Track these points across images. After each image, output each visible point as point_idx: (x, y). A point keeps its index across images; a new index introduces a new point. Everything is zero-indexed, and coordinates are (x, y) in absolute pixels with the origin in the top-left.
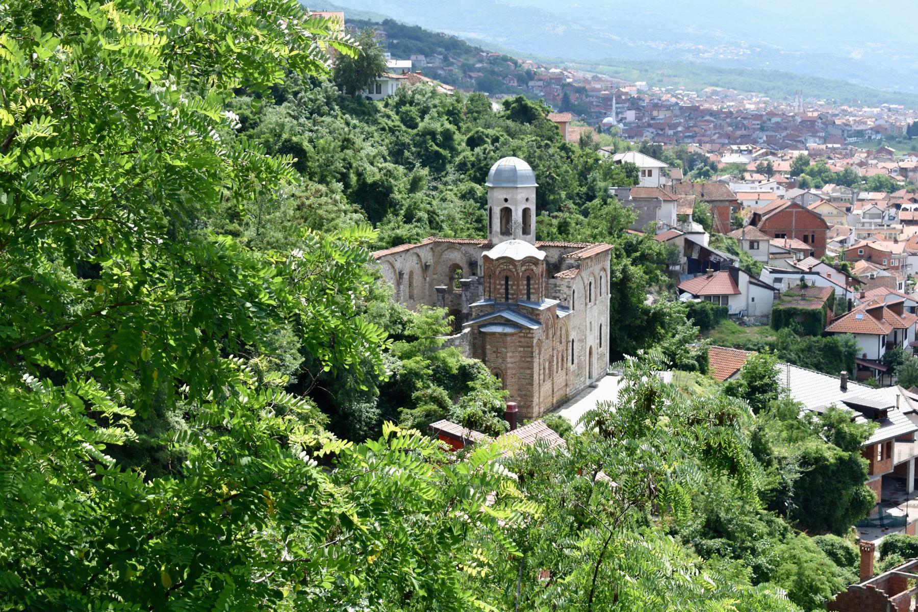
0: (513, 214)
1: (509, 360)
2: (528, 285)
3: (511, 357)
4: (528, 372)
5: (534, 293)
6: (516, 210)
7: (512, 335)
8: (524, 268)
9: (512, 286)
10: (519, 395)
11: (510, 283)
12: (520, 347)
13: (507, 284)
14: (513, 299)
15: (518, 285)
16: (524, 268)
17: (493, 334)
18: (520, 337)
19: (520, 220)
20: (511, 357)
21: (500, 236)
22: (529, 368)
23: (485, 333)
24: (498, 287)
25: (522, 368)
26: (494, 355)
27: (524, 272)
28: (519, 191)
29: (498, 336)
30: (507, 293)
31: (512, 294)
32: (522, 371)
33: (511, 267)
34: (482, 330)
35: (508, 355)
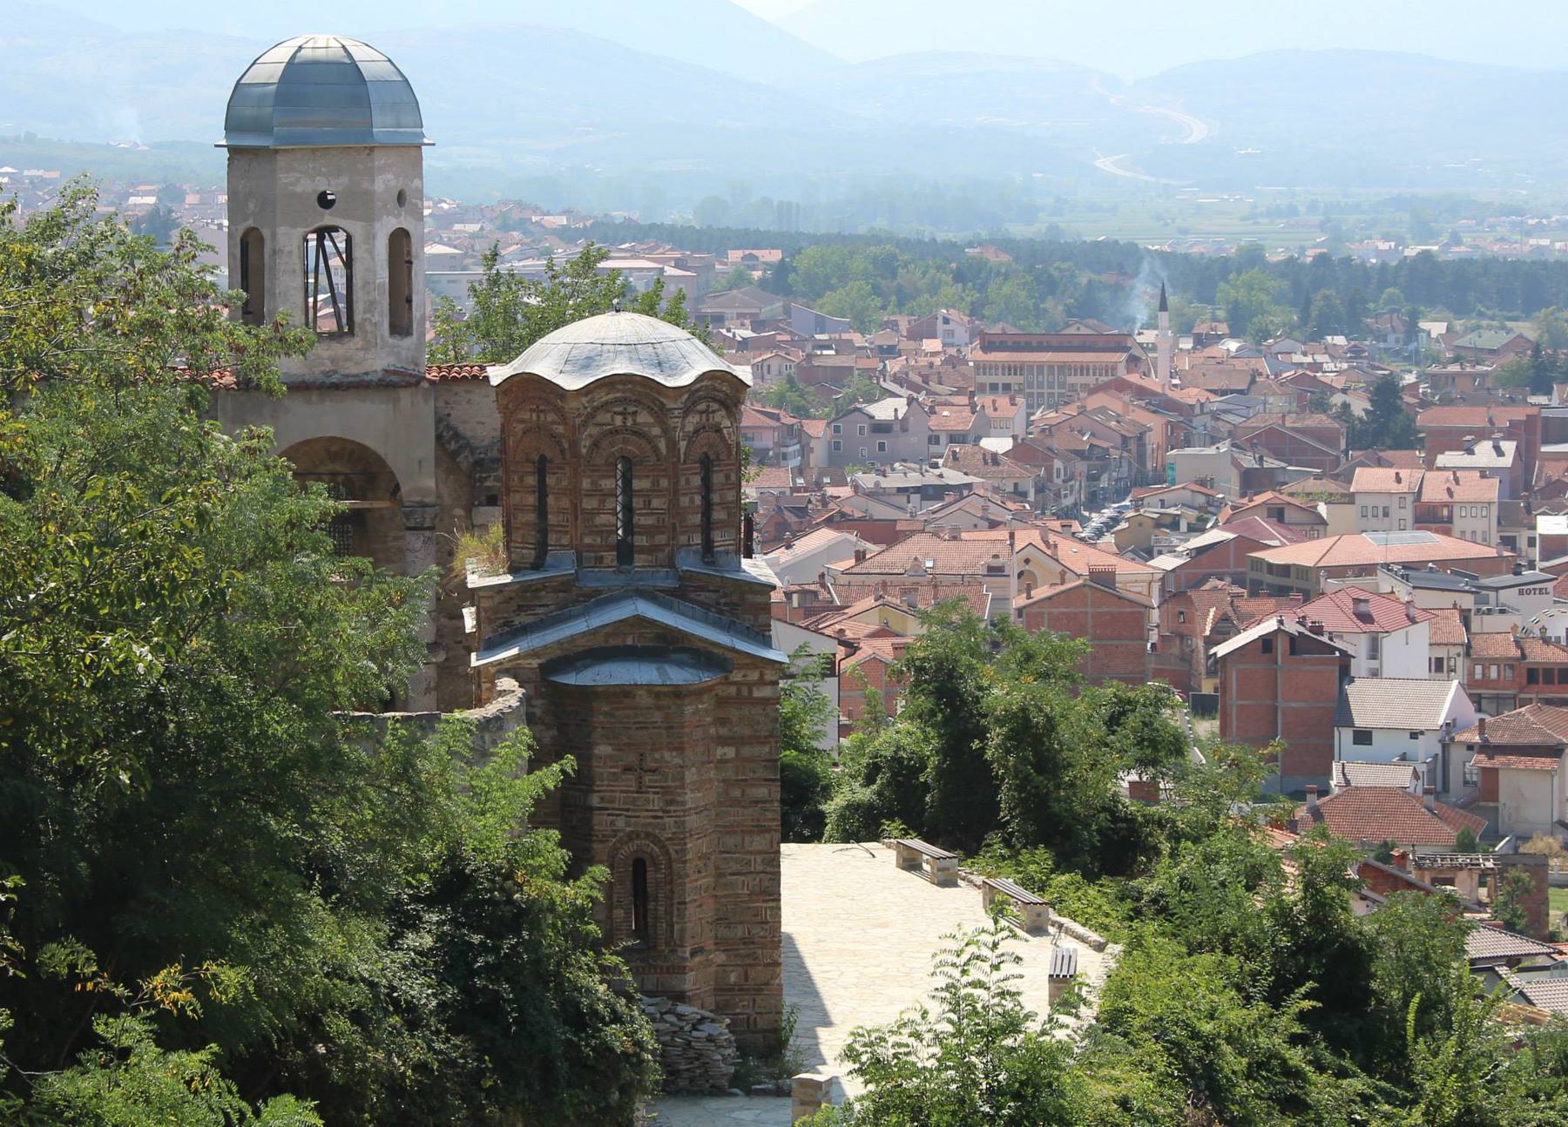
1: (691, 798)
2: (707, 487)
5: (723, 525)
6: (370, 237)
7: (698, 693)
8: (693, 421)
9: (647, 496)
10: (720, 943)
11: (637, 484)
12: (722, 741)
14: (652, 549)
15: (675, 492)
16: (693, 421)
17: (624, 693)
18: (722, 702)
19: (383, 275)
23: (587, 694)
24: (590, 504)
25: (730, 830)
26: (630, 781)
28: (380, 159)
29: (645, 700)
31: (650, 531)
32: (731, 841)
33: (644, 418)
34: (570, 679)
35: (691, 775)
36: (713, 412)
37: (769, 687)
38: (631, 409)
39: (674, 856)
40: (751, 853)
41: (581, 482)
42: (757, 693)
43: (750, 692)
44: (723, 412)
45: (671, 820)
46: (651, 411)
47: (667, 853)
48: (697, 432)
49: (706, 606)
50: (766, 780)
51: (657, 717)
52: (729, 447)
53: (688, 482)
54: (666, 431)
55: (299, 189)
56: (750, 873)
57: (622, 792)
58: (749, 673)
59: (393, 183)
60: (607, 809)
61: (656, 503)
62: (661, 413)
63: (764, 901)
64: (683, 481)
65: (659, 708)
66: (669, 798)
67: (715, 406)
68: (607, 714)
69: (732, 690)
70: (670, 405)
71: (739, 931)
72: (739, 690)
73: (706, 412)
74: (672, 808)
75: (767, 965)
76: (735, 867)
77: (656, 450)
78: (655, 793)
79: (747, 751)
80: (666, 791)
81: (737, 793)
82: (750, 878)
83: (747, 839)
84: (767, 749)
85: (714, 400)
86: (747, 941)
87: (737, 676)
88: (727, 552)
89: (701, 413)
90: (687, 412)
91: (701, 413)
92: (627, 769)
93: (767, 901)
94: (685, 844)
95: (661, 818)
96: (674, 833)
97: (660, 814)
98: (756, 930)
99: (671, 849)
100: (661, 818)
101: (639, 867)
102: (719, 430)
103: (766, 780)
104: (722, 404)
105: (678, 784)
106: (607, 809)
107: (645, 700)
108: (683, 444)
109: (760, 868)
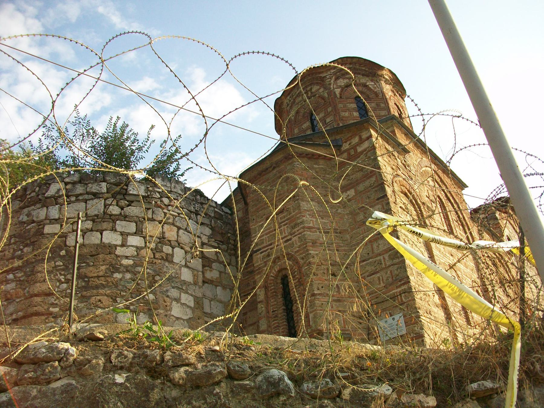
37: (366, 142)
39: (301, 262)
40: (380, 255)
41: (294, 132)
42: (359, 149)
43: (356, 151)
45: (296, 238)
46: (317, 84)
47: (297, 262)
50: (378, 199)
53: (345, 106)
56: (383, 269)
57: (266, 234)
58: (352, 140)
60: (260, 249)
61: (328, 120)
63: (397, 287)
64: (341, 106)
66: (292, 224)
72: (349, 154)
74: (296, 230)
78: (285, 225)
79: (361, 187)
82: (382, 273)
83: (375, 246)
84: (373, 179)
90: (337, 79)
93: (400, 286)
94: (308, 250)
95: (290, 239)
96: (299, 247)
97: (289, 238)
100: (290, 239)
103: (378, 199)
105: (297, 211)
106: (260, 249)
108: (338, 91)
109: (388, 264)
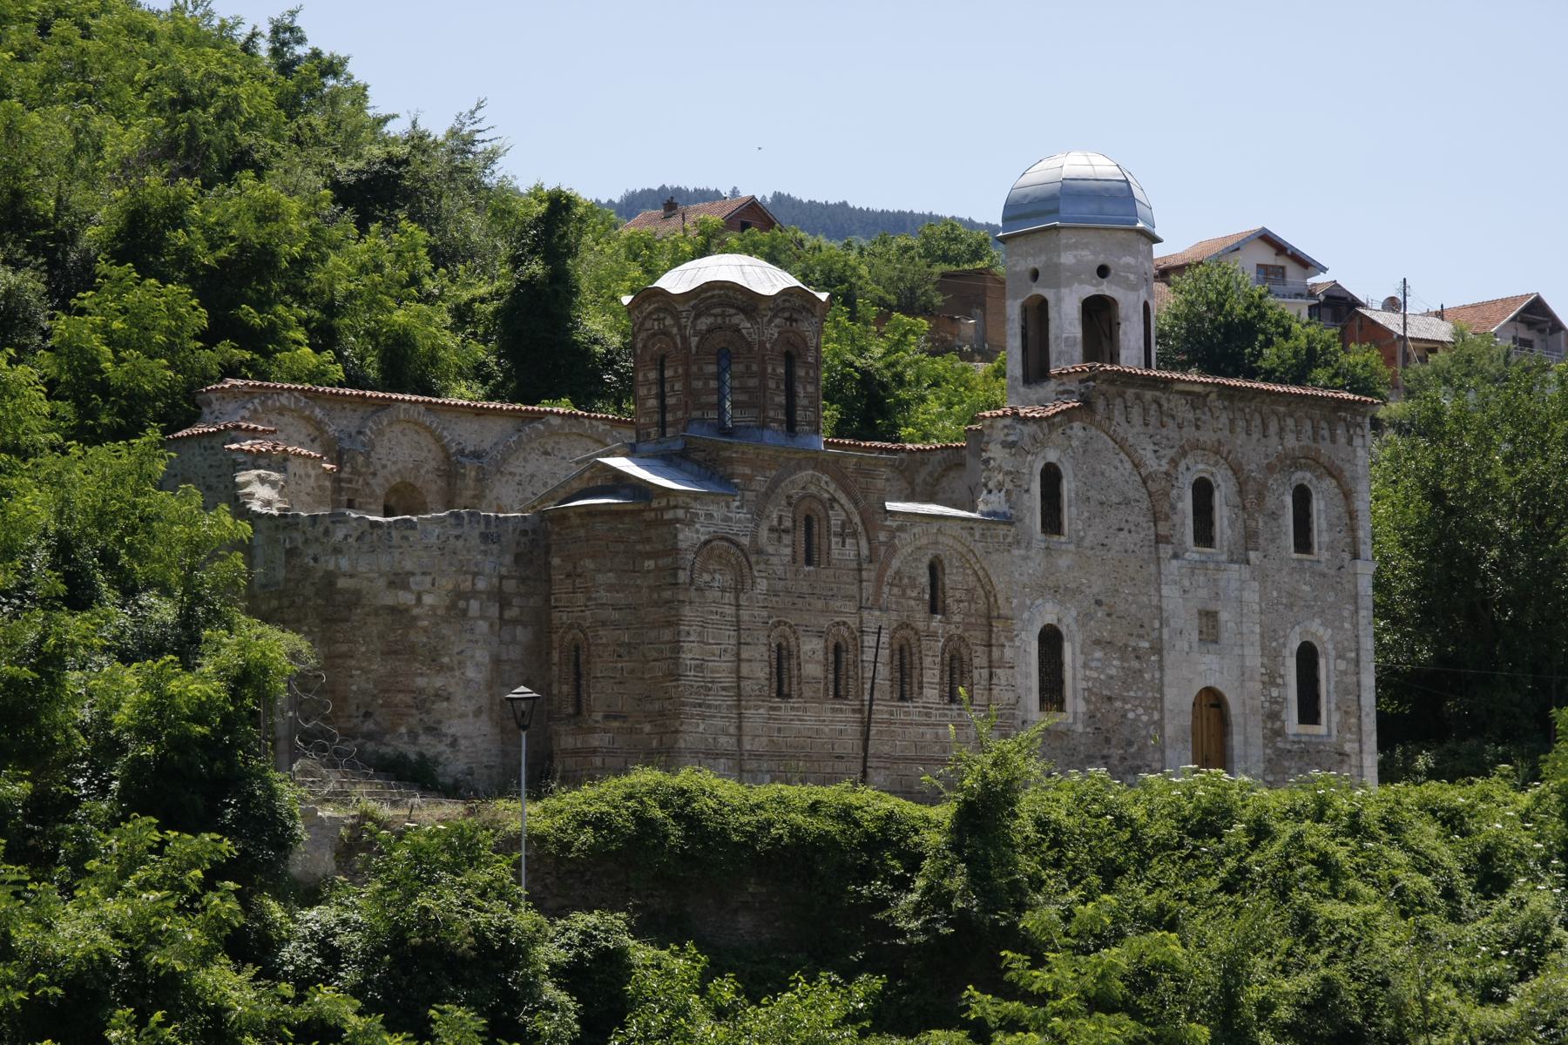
0: (1052, 314)
3: (611, 588)
4: (667, 635)
6: (1059, 300)
8: (704, 323)
13: (662, 381)
20: (611, 588)
21: (1022, 389)
22: (669, 624)
27: (704, 336)
28: (1065, 238)
30: (663, 408)
32: (653, 634)
36: (730, 316)
38: (662, 315)
40: (663, 643)
42: (666, 517)
44: (742, 316)
48: (709, 331)
49: (699, 464)
51: (582, 533)
52: (749, 345)
53: (701, 369)
54: (681, 328)
55: (1018, 269)
59: (1091, 257)
62: (676, 316)
64: (694, 369)
65: (583, 526)
67: (732, 311)
68: (558, 534)
69: (653, 514)
70: (680, 308)
71: (657, 706)
73: (723, 315)
75: (673, 732)
76: (655, 654)
77: (675, 344)
79: (661, 562)
80: (587, 590)
81: (655, 596)
84: (670, 559)
85: (732, 306)
86: (661, 713)
87: (655, 504)
88: (748, 427)
89: (715, 316)
90: (697, 317)
91: (715, 316)
92: (568, 576)
98: (667, 705)
99: (590, 635)
101: (577, 649)
102: (739, 331)
104: (741, 310)
107: (576, 521)
108: (694, 341)
